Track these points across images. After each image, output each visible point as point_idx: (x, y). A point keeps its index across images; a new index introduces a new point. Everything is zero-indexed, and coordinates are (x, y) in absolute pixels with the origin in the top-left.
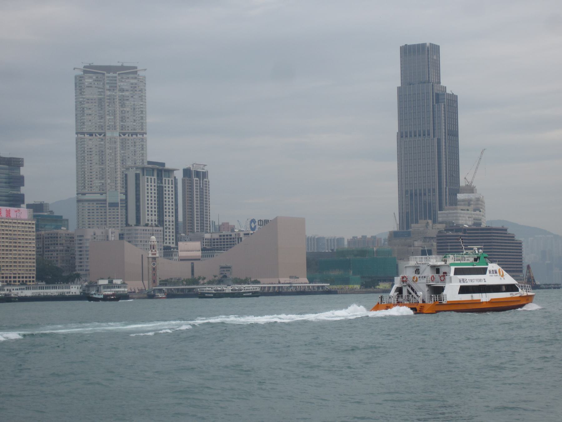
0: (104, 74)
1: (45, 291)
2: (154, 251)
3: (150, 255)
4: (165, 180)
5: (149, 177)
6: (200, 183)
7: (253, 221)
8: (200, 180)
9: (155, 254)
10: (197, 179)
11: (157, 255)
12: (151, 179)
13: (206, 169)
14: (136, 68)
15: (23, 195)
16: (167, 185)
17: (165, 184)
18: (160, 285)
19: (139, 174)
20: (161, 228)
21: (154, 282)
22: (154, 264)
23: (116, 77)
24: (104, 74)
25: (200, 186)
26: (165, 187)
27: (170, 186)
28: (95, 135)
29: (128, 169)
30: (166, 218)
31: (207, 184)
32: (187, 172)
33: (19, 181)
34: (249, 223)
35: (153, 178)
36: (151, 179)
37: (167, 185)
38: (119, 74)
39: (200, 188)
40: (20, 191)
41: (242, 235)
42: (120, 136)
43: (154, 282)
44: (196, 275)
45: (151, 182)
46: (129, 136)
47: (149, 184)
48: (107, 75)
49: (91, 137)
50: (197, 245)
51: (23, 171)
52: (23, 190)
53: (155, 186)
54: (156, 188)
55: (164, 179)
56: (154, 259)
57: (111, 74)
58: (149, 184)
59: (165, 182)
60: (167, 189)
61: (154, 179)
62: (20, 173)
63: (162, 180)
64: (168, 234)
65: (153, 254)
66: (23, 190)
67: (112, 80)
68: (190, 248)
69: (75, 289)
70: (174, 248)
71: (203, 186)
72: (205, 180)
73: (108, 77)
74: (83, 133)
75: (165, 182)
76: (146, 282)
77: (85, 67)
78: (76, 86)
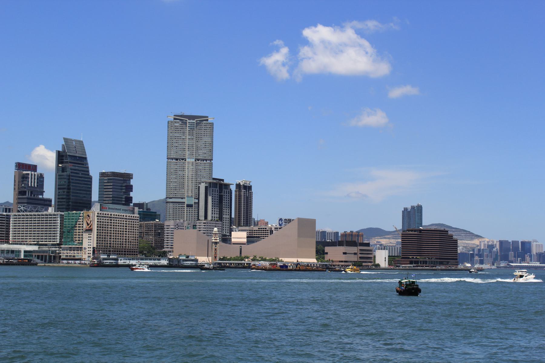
1: (144, 261)
3: (214, 241)
7: (281, 220)
11: (218, 241)
13: (251, 184)
14: (207, 117)
16: (225, 194)
18: (220, 259)
20: (221, 223)
21: (215, 257)
22: (216, 246)
27: (228, 195)
29: (200, 183)
30: (224, 216)
31: (251, 194)
32: (238, 186)
33: (130, 188)
34: (278, 221)
37: (225, 194)
41: (273, 229)
43: (215, 257)
44: (243, 255)
47: (214, 193)
48: (188, 121)
49: (176, 161)
50: (244, 234)
51: (132, 182)
52: (132, 194)
56: (216, 243)
57: (191, 121)
58: (214, 193)
60: (225, 197)
64: (225, 226)
66: (132, 194)
68: (239, 236)
69: (164, 262)
70: (228, 236)
74: (172, 159)
76: (210, 258)
77: (175, 116)
78: (168, 128)
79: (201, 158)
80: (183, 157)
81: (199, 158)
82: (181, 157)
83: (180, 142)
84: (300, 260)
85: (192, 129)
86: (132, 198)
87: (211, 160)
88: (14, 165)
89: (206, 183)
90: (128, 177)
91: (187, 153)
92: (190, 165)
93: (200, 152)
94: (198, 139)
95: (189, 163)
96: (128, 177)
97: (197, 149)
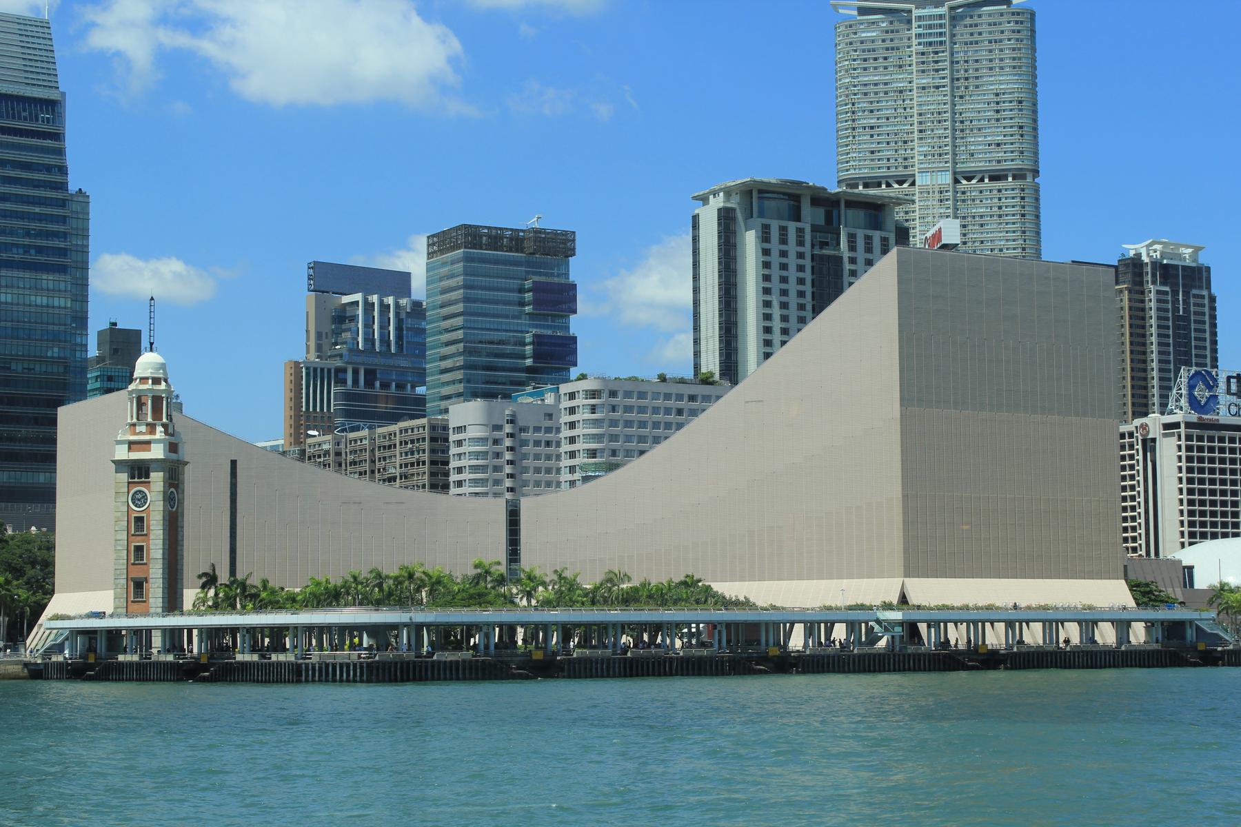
0: (910, 11)
3: (122, 453)
6: (1175, 301)
8: (1175, 293)
10: (1167, 289)
11: (157, 452)
12: (783, 230)
13: (1203, 260)
15: (574, 339)
19: (733, 210)
22: (139, 499)
23: (941, 17)
24: (910, 11)
25: (1176, 309)
28: (889, 185)
29: (704, 199)
35: (792, 226)
36: (783, 230)
38: (952, 8)
39: (1177, 318)
40: (567, 328)
42: (956, 181)
45: (784, 241)
46: (982, 180)
47: (775, 246)
48: (916, 12)
52: (576, 325)
54: (807, 263)
56: (139, 470)
61: (800, 231)
62: (567, 275)
67: (930, 27)
71: (1186, 310)
72: (1195, 292)
73: (919, 18)
79: (982, 165)
80: (901, 171)
81: (972, 166)
82: (893, 172)
83: (887, 106)
84: (931, 592)
85: (932, 46)
86: (574, 340)
87: (1036, 172)
88: (304, 272)
89: (728, 192)
90: (556, 246)
91: (918, 149)
92: (933, 201)
93: (976, 142)
94: (959, 84)
95: (926, 192)
96: (556, 246)
97: (959, 128)
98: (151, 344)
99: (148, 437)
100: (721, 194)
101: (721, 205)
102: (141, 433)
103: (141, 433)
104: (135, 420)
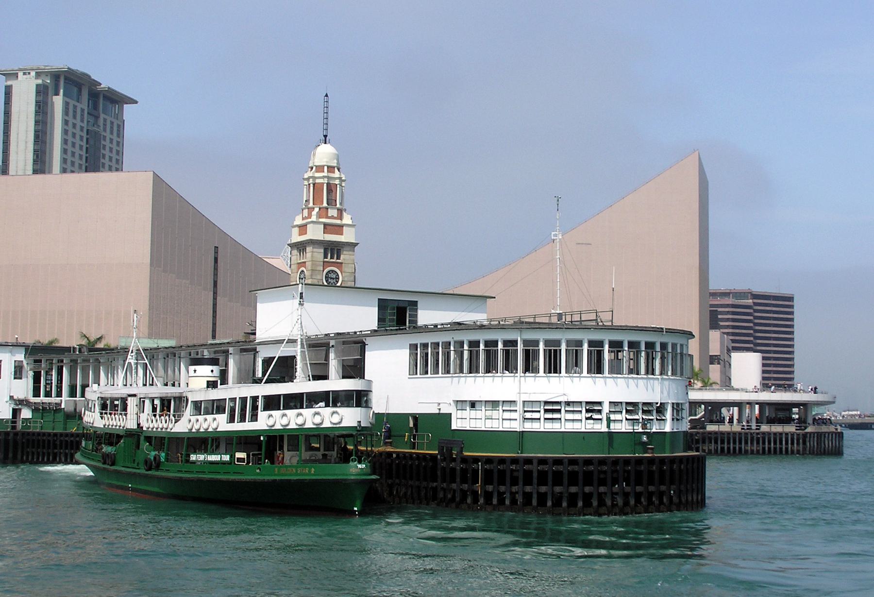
2: (333, 212)
4: (105, 120)
5: (72, 103)
9: (338, 229)
12: (75, 107)
16: (108, 136)
17: (105, 130)
26: (105, 137)
35: (79, 106)
53: (82, 129)
54: (84, 134)
55: (102, 116)
59: (105, 125)
61: (82, 110)
63: (97, 118)
65: (327, 228)
75: (105, 125)
98: (325, 136)
99: (338, 222)
100: (33, 73)
101: (40, 81)
102: (332, 217)
103: (332, 217)
104: (325, 204)
